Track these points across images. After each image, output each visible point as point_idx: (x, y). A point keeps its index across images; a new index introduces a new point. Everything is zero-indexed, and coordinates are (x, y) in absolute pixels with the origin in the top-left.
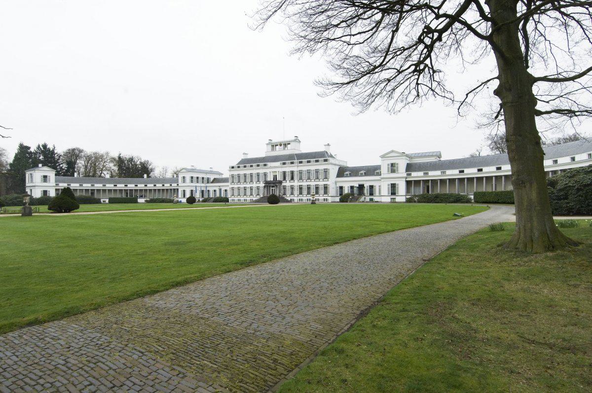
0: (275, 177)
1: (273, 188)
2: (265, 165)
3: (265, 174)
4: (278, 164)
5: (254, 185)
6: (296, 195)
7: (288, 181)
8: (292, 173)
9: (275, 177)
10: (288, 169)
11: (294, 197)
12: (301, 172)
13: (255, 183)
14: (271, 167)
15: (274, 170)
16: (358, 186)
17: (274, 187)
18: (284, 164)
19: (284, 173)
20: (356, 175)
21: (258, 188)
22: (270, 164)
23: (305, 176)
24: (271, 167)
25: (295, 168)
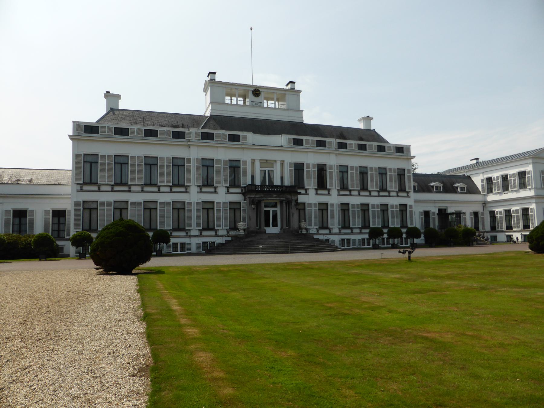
0: (267, 176)
1: (271, 209)
2: (234, 138)
3: (234, 167)
4: (282, 140)
5: (194, 196)
6: (336, 230)
7: (312, 192)
8: (321, 170)
9: (267, 176)
10: (311, 158)
11: (330, 233)
12: (344, 171)
13: (194, 190)
14: (254, 147)
15: (270, 158)
16: (437, 212)
17: (275, 206)
18: (298, 142)
19: (299, 169)
20: (429, 190)
21: (208, 208)
22: (251, 137)
23: (354, 183)
24: (254, 147)
25: (332, 159)
